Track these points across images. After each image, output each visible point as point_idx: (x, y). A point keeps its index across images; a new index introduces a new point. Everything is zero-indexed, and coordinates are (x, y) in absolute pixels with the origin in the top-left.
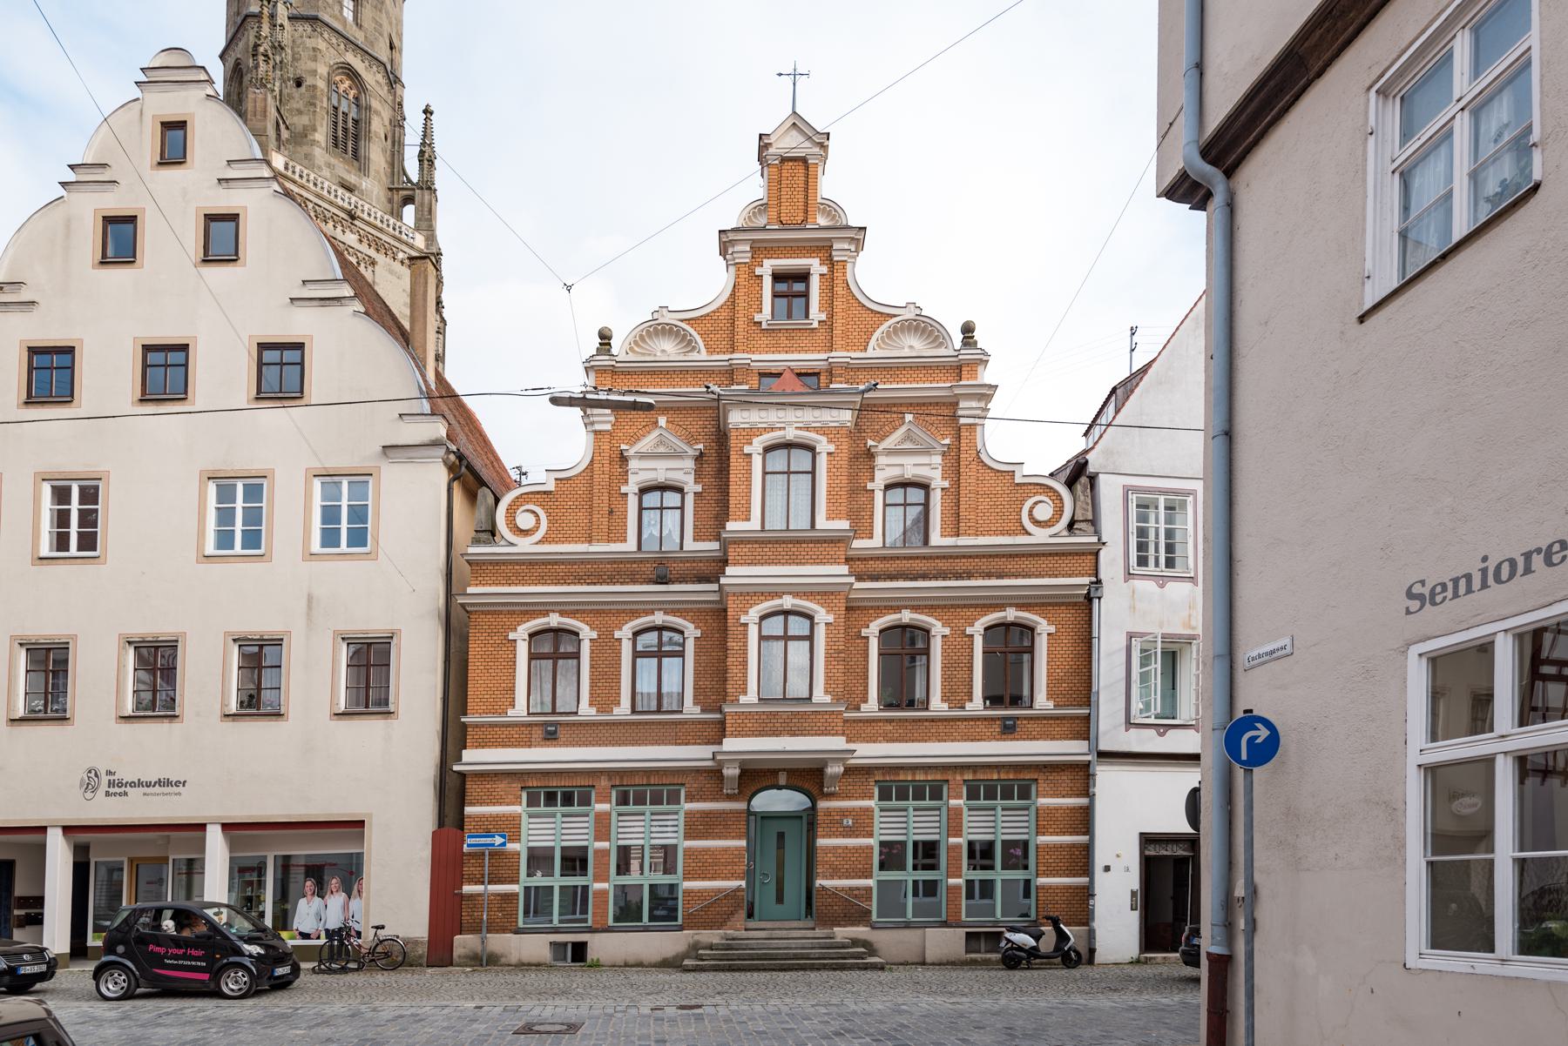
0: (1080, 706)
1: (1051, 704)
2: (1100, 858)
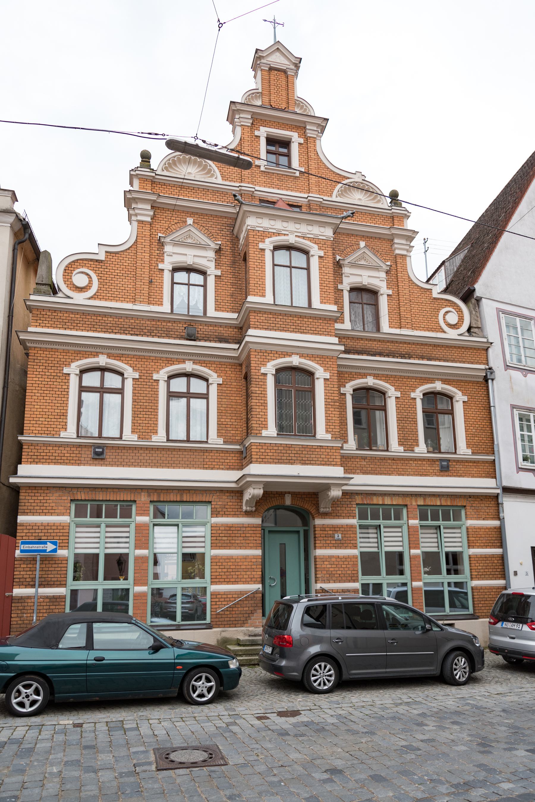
0: (487, 454)
1: (469, 451)
2: (513, 565)
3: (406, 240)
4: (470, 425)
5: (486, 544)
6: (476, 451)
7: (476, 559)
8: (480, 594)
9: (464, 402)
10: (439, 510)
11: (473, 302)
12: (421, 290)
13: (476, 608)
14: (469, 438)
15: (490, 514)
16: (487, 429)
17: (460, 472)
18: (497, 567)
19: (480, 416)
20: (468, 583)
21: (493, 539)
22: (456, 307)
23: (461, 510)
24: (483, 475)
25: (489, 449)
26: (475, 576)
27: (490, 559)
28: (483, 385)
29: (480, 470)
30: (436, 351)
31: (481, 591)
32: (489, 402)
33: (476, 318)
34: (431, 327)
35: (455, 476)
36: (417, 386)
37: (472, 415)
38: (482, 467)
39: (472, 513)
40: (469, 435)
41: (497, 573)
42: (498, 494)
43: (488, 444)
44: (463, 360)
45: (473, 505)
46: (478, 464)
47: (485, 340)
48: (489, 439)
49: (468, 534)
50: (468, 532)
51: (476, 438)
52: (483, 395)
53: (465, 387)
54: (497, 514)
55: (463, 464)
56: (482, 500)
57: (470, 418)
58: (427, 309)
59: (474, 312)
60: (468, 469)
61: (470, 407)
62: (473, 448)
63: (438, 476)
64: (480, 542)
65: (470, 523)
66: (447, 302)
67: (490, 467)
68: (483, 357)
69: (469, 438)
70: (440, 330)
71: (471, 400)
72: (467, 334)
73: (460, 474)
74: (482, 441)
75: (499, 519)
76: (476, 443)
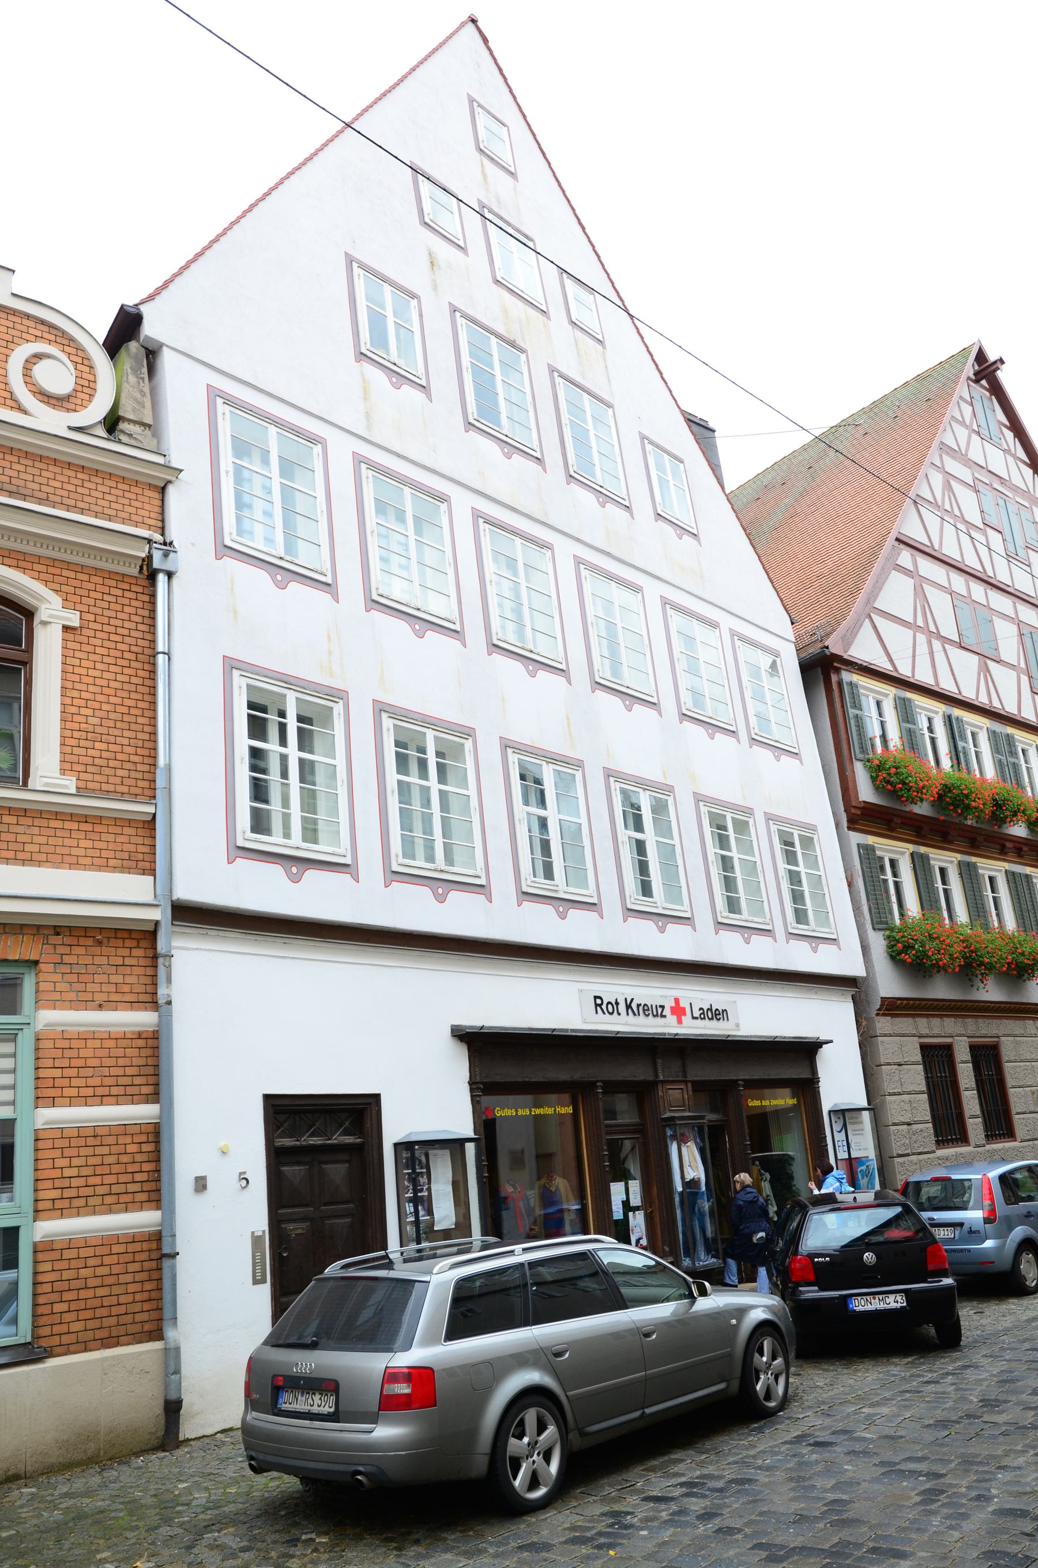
1: (70, 784)
5: (100, 1091)
6: (97, 786)
7: (58, 1143)
8: (64, 1265)
9: (66, 628)
15: (126, 989)
16: (140, 720)
19: (119, 677)
20: (22, 1233)
21: (129, 1071)
24: (112, 862)
25: (141, 784)
26: (48, 1205)
27: (112, 1140)
28: (140, 589)
29: (103, 845)
32: (153, 641)
33: (138, 396)
37: (91, 672)
38: (111, 838)
39: (59, 987)
41: (132, 1188)
42: (157, 923)
43: (140, 767)
45: (66, 959)
46: (97, 828)
51: (97, 745)
53: (77, 583)
54: (149, 989)
55: (44, 823)
56: (100, 943)
57: (85, 679)
60: (60, 841)
62: (83, 776)
64: (81, 1082)
65: (49, 1018)
67: (140, 840)
68: (147, 507)
72: (101, 432)
74: (119, 756)
75: (152, 1002)
76: (97, 761)
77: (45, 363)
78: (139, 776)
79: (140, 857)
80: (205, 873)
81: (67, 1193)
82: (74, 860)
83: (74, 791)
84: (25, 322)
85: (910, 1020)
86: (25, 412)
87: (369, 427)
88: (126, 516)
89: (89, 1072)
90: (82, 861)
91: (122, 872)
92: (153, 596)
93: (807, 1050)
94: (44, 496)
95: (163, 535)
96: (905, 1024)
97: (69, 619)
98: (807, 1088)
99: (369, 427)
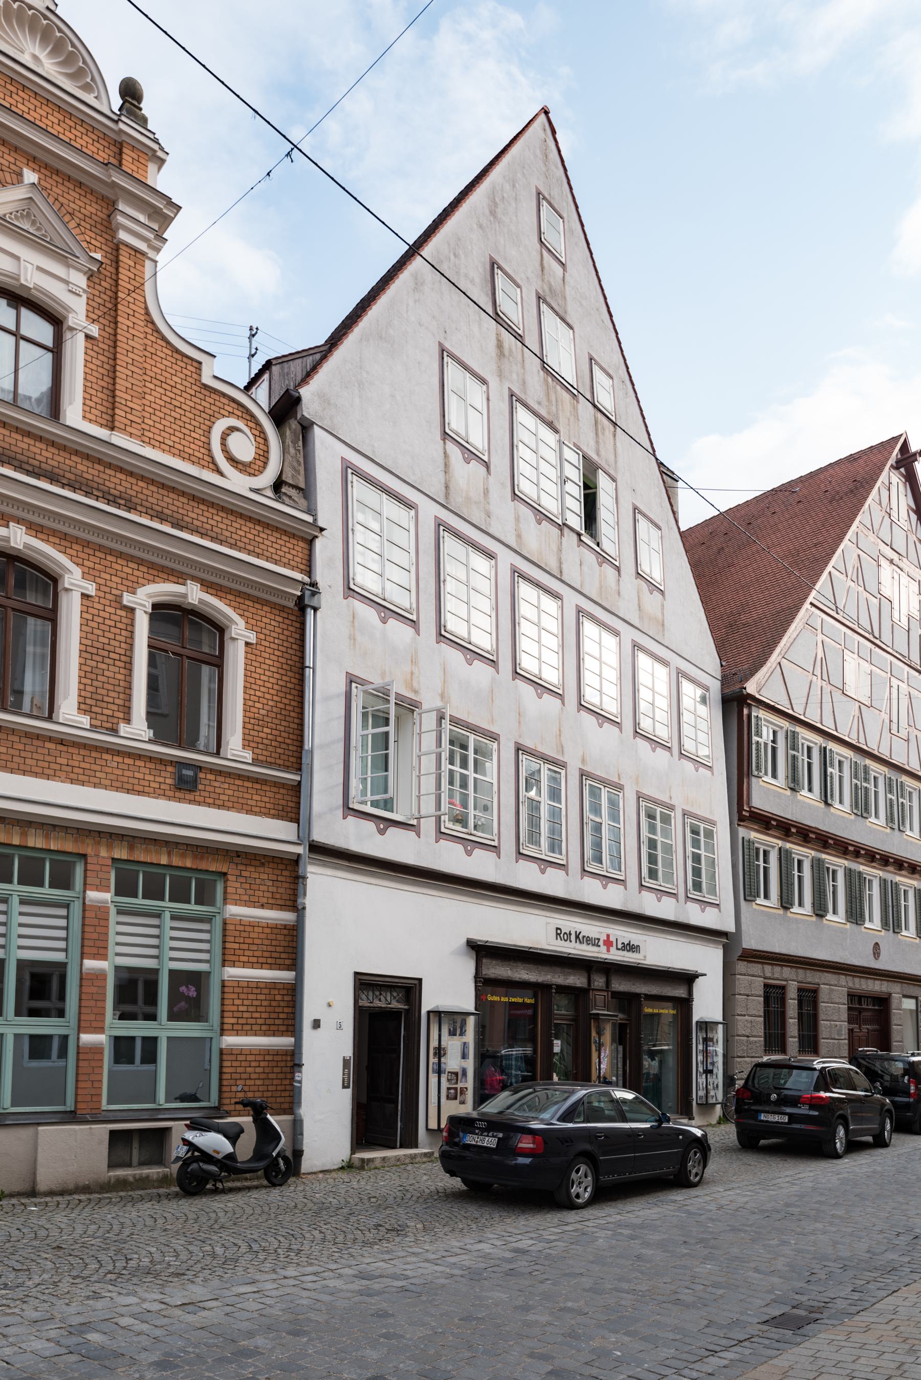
0: (286, 768)
1: (248, 756)
2: (310, 1009)
3: (150, 217)
4: (256, 699)
5: (261, 960)
6: (264, 758)
7: (236, 990)
8: (237, 1064)
10: (165, 875)
11: (294, 426)
12: (175, 355)
13: (225, 1095)
14: (250, 726)
15: (278, 896)
17: (222, 797)
18: (280, 1010)
20: (214, 1041)
21: (278, 949)
22: (253, 425)
23: (216, 880)
24: (272, 812)
26: (230, 1027)
28: (294, 618)
30: (196, 510)
31: (240, 1058)
33: (295, 464)
34: (191, 452)
35: (209, 805)
36: (141, 580)
37: (263, 677)
40: (252, 721)
41: (277, 1022)
42: (299, 855)
43: (291, 748)
44: (257, 550)
45: (244, 873)
46: (264, 788)
47: (310, 519)
48: (295, 737)
49: (224, 936)
50: (224, 930)
51: (265, 730)
52: (290, 640)
54: (292, 898)
57: (259, 682)
58: (184, 406)
59: (292, 451)
60: (241, 794)
61: (261, 660)
62: (256, 751)
63: (169, 798)
64: (250, 953)
65: (234, 910)
66: (235, 406)
67: (289, 798)
69: (250, 726)
70: (211, 466)
71: (263, 643)
73: (220, 803)
74: (279, 739)
77: (236, 435)
78: (291, 754)
79: (289, 809)
80: (331, 827)
81: (241, 1021)
82: (249, 808)
83: (250, 761)
84: (223, 400)
85: (760, 966)
86: (221, 474)
87: (447, 495)
88: (286, 561)
89: (255, 947)
90: (254, 809)
91: (278, 819)
92: (303, 624)
93: (688, 979)
94: (233, 542)
95: (310, 577)
96: (756, 968)
97: (249, 637)
98: (685, 1005)
99: (447, 495)
